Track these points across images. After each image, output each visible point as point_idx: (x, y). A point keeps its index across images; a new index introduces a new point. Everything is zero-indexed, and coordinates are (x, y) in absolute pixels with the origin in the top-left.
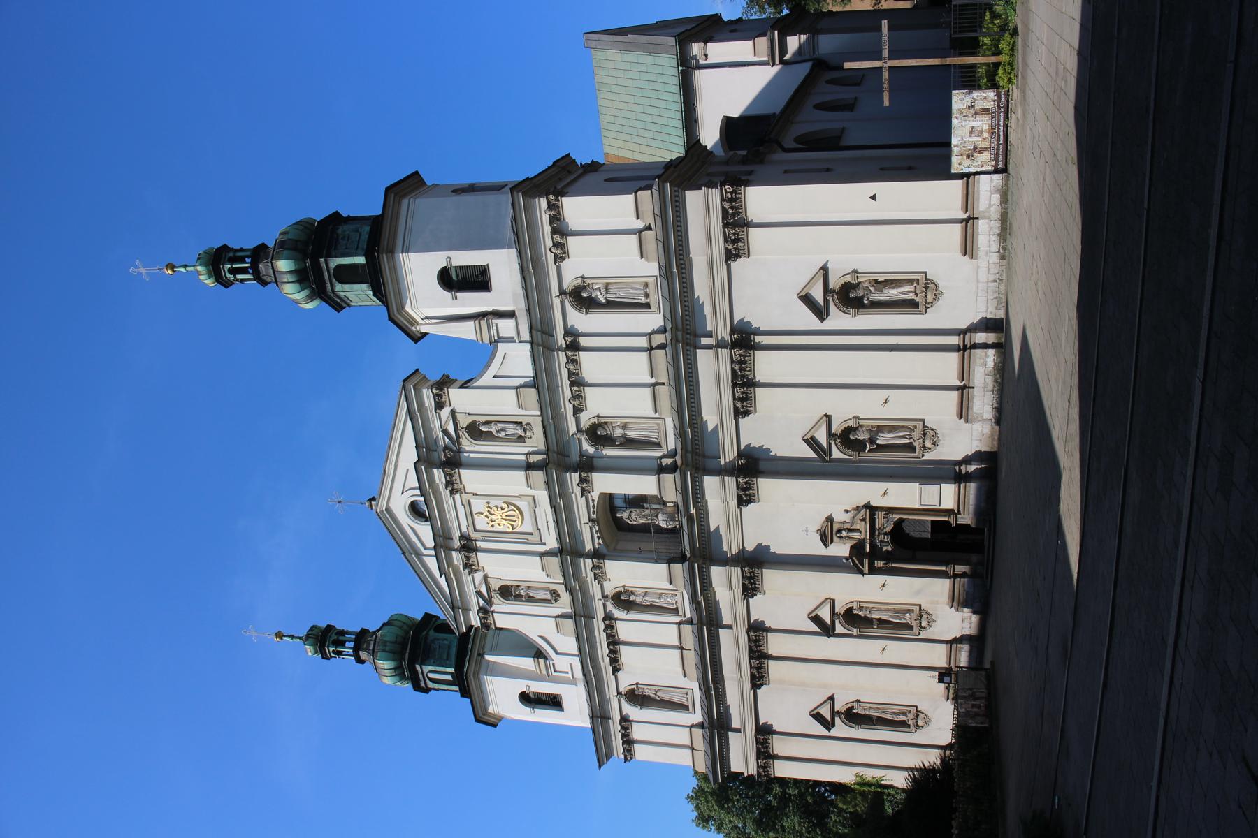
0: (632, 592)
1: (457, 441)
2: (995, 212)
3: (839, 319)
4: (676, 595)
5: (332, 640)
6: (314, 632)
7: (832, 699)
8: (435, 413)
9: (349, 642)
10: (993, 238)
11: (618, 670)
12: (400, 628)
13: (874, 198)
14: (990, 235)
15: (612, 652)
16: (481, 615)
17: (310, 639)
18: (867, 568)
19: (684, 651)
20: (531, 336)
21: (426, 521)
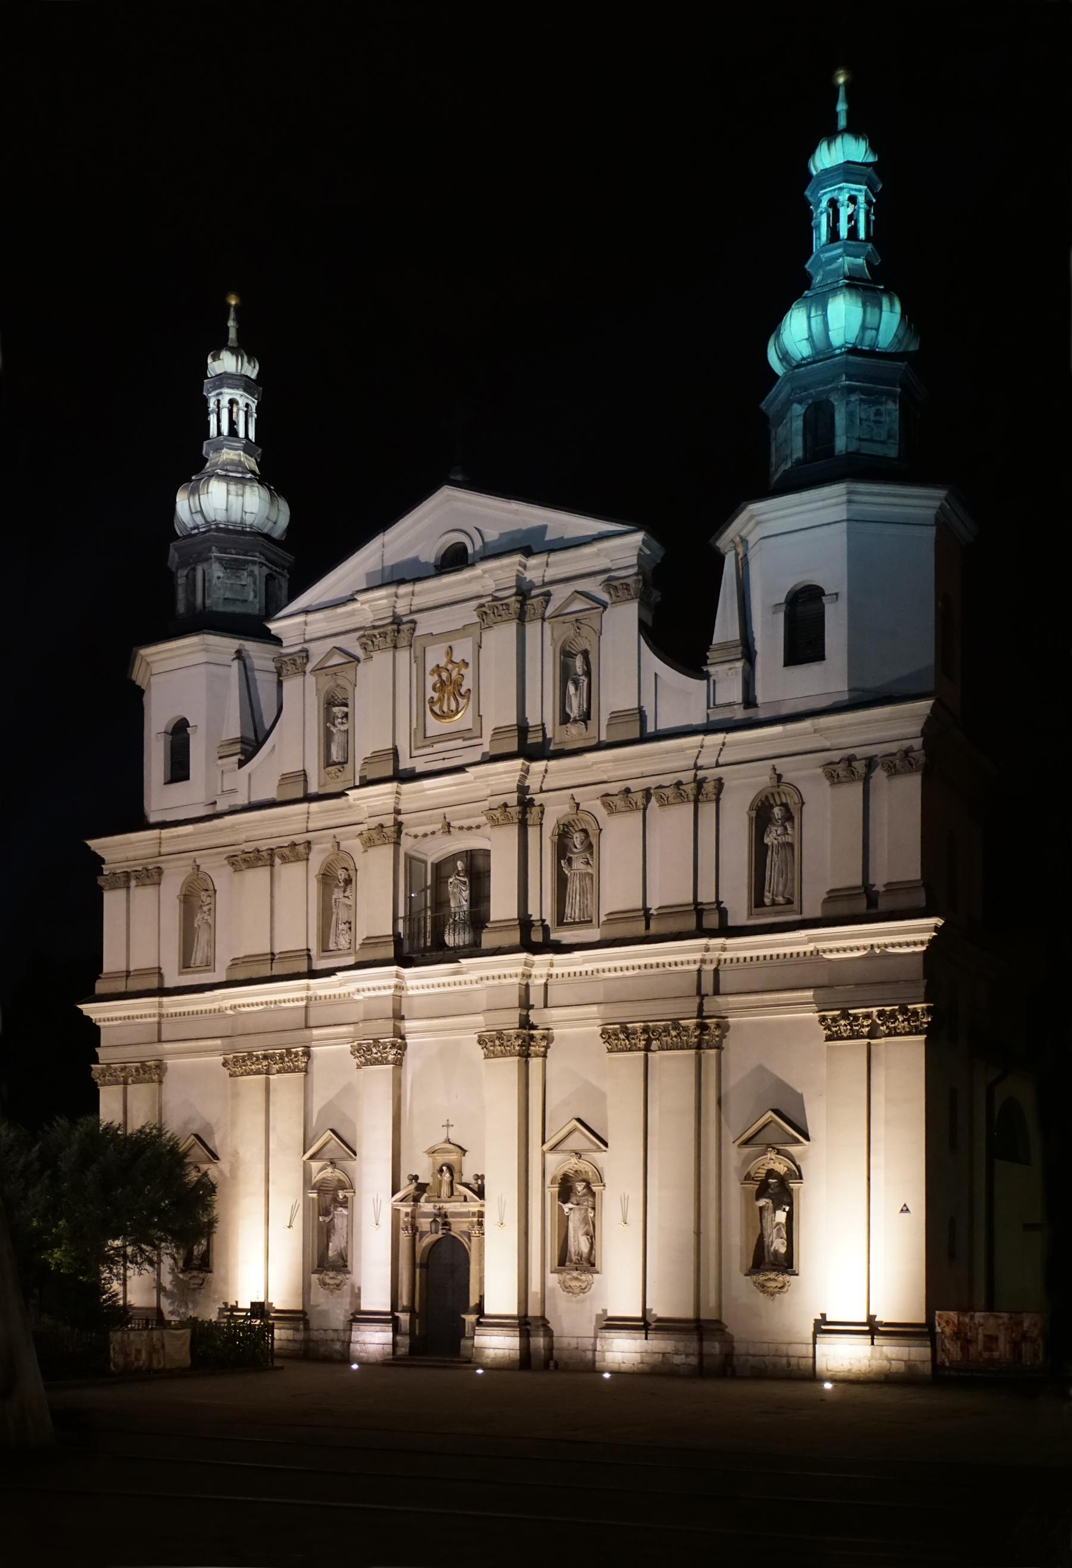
0: (348, 881)
4: (350, 948)
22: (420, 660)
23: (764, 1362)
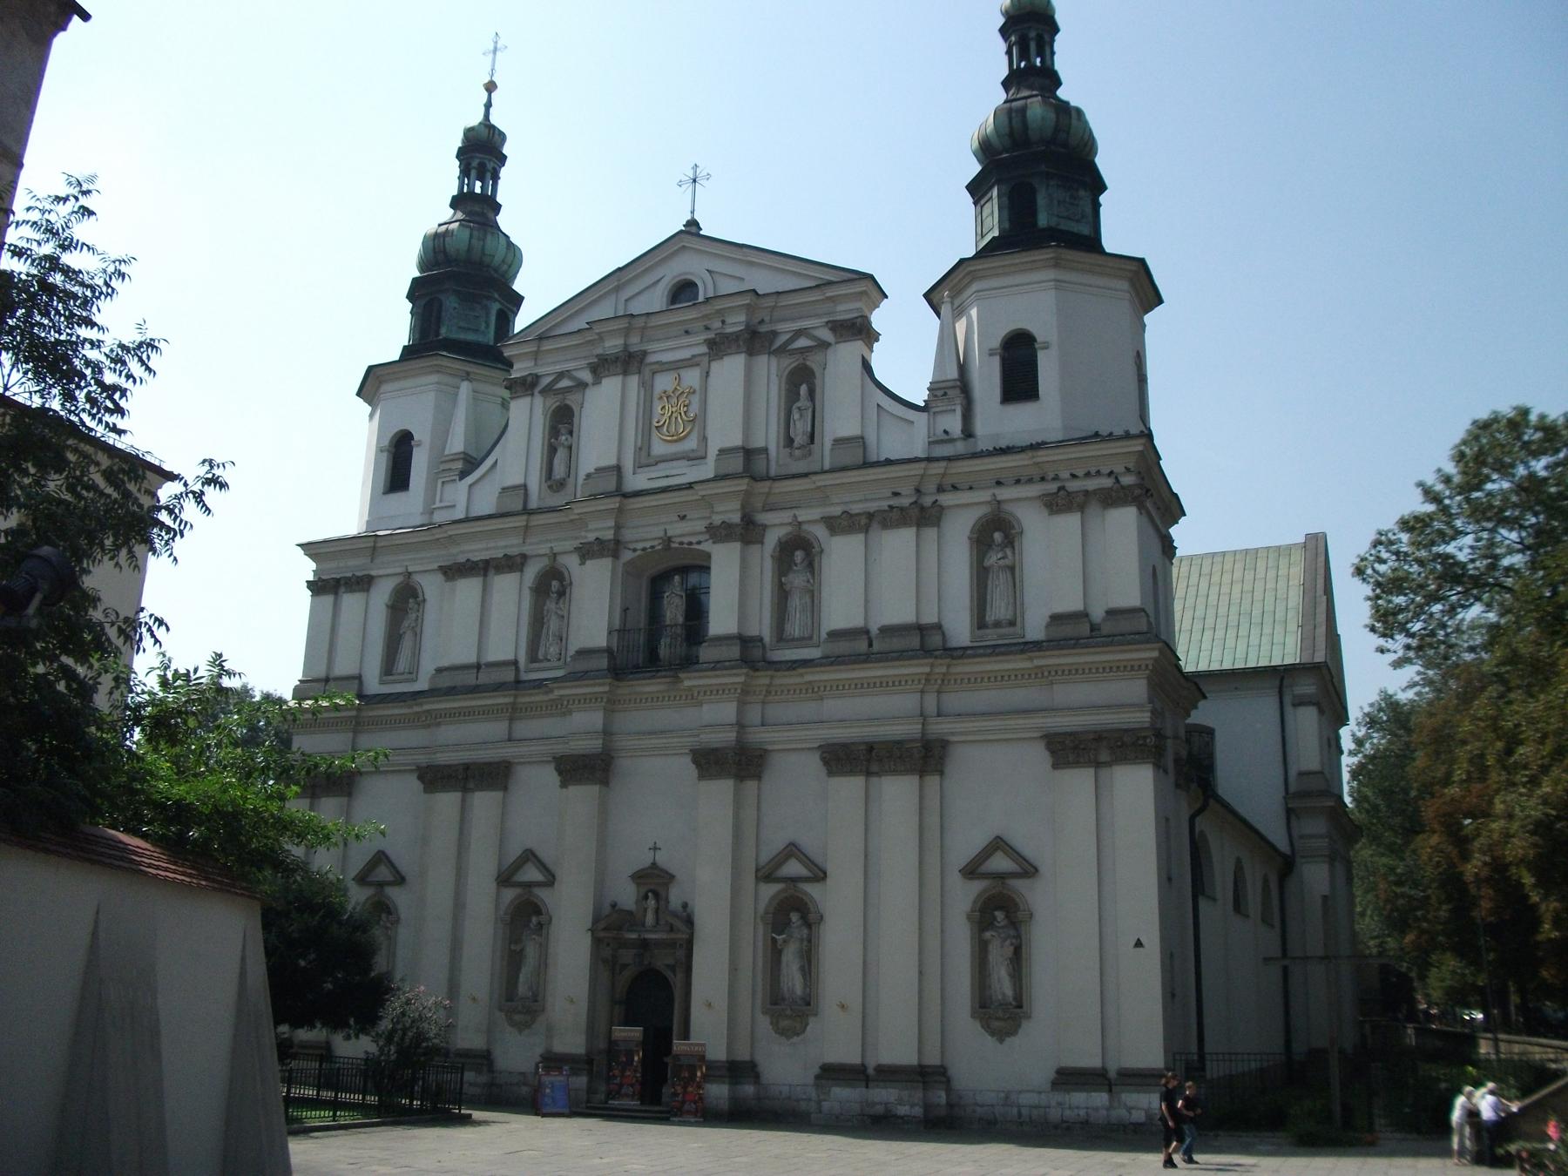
0: (562, 594)
1: (782, 350)
2: (1120, 1113)
3: (965, 895)
5: (487, 162)
6: (496, 136)
7: (400, 880)
8: (826, 320)
9: (482, 187)
10: (1082, 1113)
11: (445, 574)
12: (503, 261)
13: (1139, 944)
14: (1087, 1108)
15: (476, 563)
16: (529, 379)
17: (487, 131)
18: (602, 934)
19: (475, 671)
20: (937, 459)
21: (667, 305)
22: (647, 386)
23: (993, 1113)
